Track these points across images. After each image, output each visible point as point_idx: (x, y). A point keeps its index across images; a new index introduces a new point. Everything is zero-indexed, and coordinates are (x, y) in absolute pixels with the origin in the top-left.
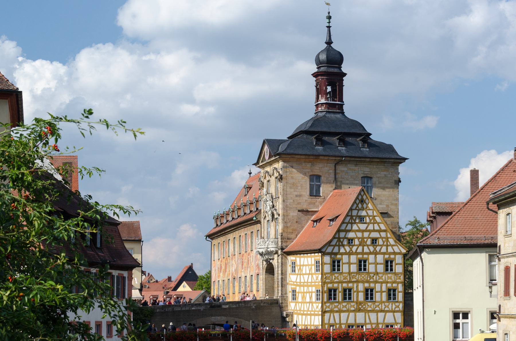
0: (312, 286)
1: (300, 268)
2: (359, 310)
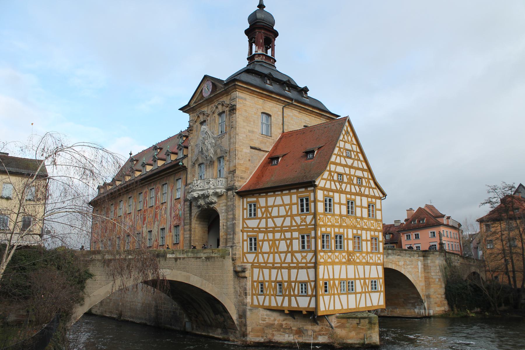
0: (291, 231)
1: (267, 210)
2: (349, 262)
